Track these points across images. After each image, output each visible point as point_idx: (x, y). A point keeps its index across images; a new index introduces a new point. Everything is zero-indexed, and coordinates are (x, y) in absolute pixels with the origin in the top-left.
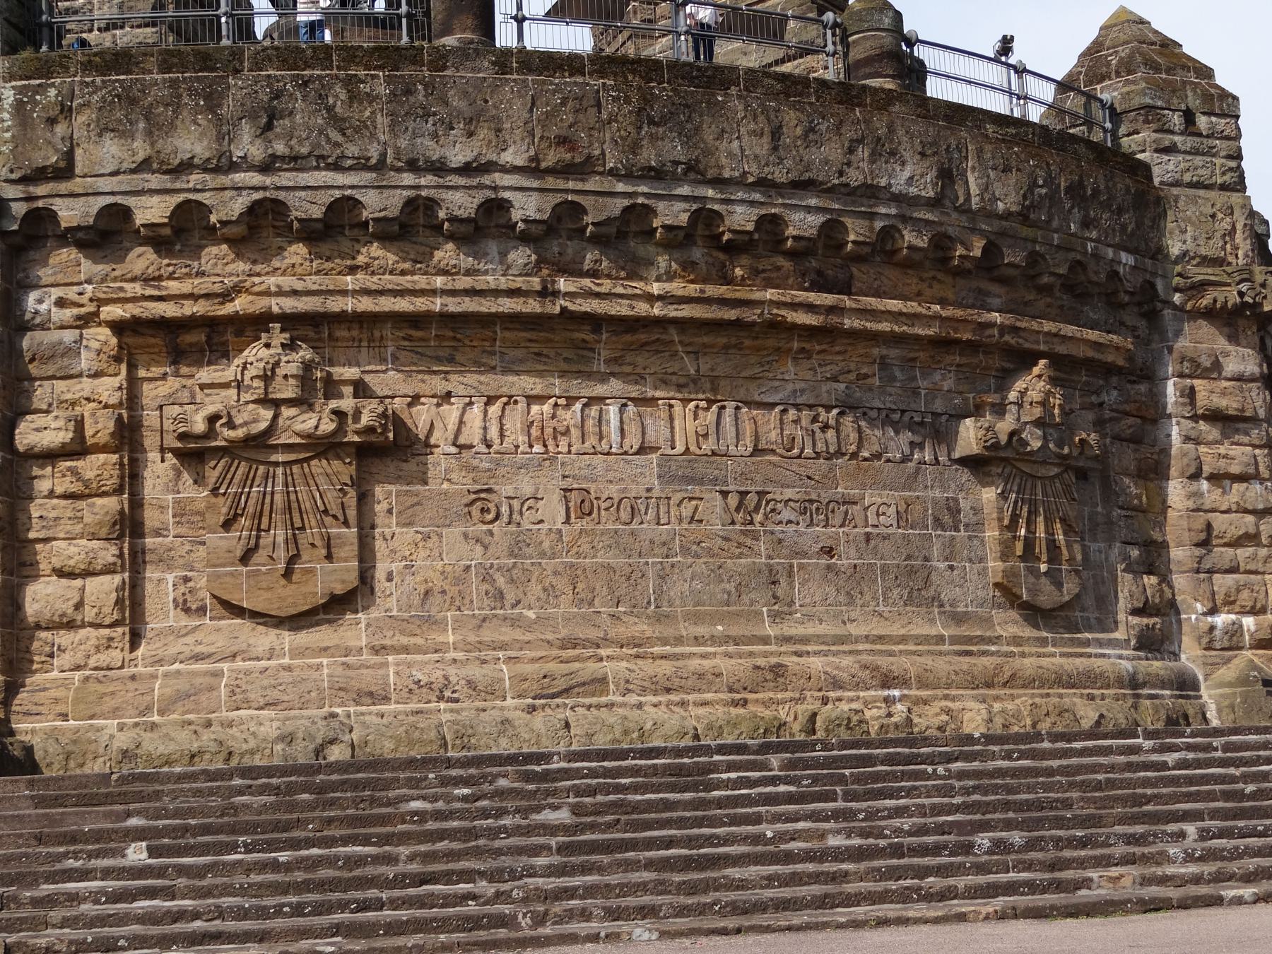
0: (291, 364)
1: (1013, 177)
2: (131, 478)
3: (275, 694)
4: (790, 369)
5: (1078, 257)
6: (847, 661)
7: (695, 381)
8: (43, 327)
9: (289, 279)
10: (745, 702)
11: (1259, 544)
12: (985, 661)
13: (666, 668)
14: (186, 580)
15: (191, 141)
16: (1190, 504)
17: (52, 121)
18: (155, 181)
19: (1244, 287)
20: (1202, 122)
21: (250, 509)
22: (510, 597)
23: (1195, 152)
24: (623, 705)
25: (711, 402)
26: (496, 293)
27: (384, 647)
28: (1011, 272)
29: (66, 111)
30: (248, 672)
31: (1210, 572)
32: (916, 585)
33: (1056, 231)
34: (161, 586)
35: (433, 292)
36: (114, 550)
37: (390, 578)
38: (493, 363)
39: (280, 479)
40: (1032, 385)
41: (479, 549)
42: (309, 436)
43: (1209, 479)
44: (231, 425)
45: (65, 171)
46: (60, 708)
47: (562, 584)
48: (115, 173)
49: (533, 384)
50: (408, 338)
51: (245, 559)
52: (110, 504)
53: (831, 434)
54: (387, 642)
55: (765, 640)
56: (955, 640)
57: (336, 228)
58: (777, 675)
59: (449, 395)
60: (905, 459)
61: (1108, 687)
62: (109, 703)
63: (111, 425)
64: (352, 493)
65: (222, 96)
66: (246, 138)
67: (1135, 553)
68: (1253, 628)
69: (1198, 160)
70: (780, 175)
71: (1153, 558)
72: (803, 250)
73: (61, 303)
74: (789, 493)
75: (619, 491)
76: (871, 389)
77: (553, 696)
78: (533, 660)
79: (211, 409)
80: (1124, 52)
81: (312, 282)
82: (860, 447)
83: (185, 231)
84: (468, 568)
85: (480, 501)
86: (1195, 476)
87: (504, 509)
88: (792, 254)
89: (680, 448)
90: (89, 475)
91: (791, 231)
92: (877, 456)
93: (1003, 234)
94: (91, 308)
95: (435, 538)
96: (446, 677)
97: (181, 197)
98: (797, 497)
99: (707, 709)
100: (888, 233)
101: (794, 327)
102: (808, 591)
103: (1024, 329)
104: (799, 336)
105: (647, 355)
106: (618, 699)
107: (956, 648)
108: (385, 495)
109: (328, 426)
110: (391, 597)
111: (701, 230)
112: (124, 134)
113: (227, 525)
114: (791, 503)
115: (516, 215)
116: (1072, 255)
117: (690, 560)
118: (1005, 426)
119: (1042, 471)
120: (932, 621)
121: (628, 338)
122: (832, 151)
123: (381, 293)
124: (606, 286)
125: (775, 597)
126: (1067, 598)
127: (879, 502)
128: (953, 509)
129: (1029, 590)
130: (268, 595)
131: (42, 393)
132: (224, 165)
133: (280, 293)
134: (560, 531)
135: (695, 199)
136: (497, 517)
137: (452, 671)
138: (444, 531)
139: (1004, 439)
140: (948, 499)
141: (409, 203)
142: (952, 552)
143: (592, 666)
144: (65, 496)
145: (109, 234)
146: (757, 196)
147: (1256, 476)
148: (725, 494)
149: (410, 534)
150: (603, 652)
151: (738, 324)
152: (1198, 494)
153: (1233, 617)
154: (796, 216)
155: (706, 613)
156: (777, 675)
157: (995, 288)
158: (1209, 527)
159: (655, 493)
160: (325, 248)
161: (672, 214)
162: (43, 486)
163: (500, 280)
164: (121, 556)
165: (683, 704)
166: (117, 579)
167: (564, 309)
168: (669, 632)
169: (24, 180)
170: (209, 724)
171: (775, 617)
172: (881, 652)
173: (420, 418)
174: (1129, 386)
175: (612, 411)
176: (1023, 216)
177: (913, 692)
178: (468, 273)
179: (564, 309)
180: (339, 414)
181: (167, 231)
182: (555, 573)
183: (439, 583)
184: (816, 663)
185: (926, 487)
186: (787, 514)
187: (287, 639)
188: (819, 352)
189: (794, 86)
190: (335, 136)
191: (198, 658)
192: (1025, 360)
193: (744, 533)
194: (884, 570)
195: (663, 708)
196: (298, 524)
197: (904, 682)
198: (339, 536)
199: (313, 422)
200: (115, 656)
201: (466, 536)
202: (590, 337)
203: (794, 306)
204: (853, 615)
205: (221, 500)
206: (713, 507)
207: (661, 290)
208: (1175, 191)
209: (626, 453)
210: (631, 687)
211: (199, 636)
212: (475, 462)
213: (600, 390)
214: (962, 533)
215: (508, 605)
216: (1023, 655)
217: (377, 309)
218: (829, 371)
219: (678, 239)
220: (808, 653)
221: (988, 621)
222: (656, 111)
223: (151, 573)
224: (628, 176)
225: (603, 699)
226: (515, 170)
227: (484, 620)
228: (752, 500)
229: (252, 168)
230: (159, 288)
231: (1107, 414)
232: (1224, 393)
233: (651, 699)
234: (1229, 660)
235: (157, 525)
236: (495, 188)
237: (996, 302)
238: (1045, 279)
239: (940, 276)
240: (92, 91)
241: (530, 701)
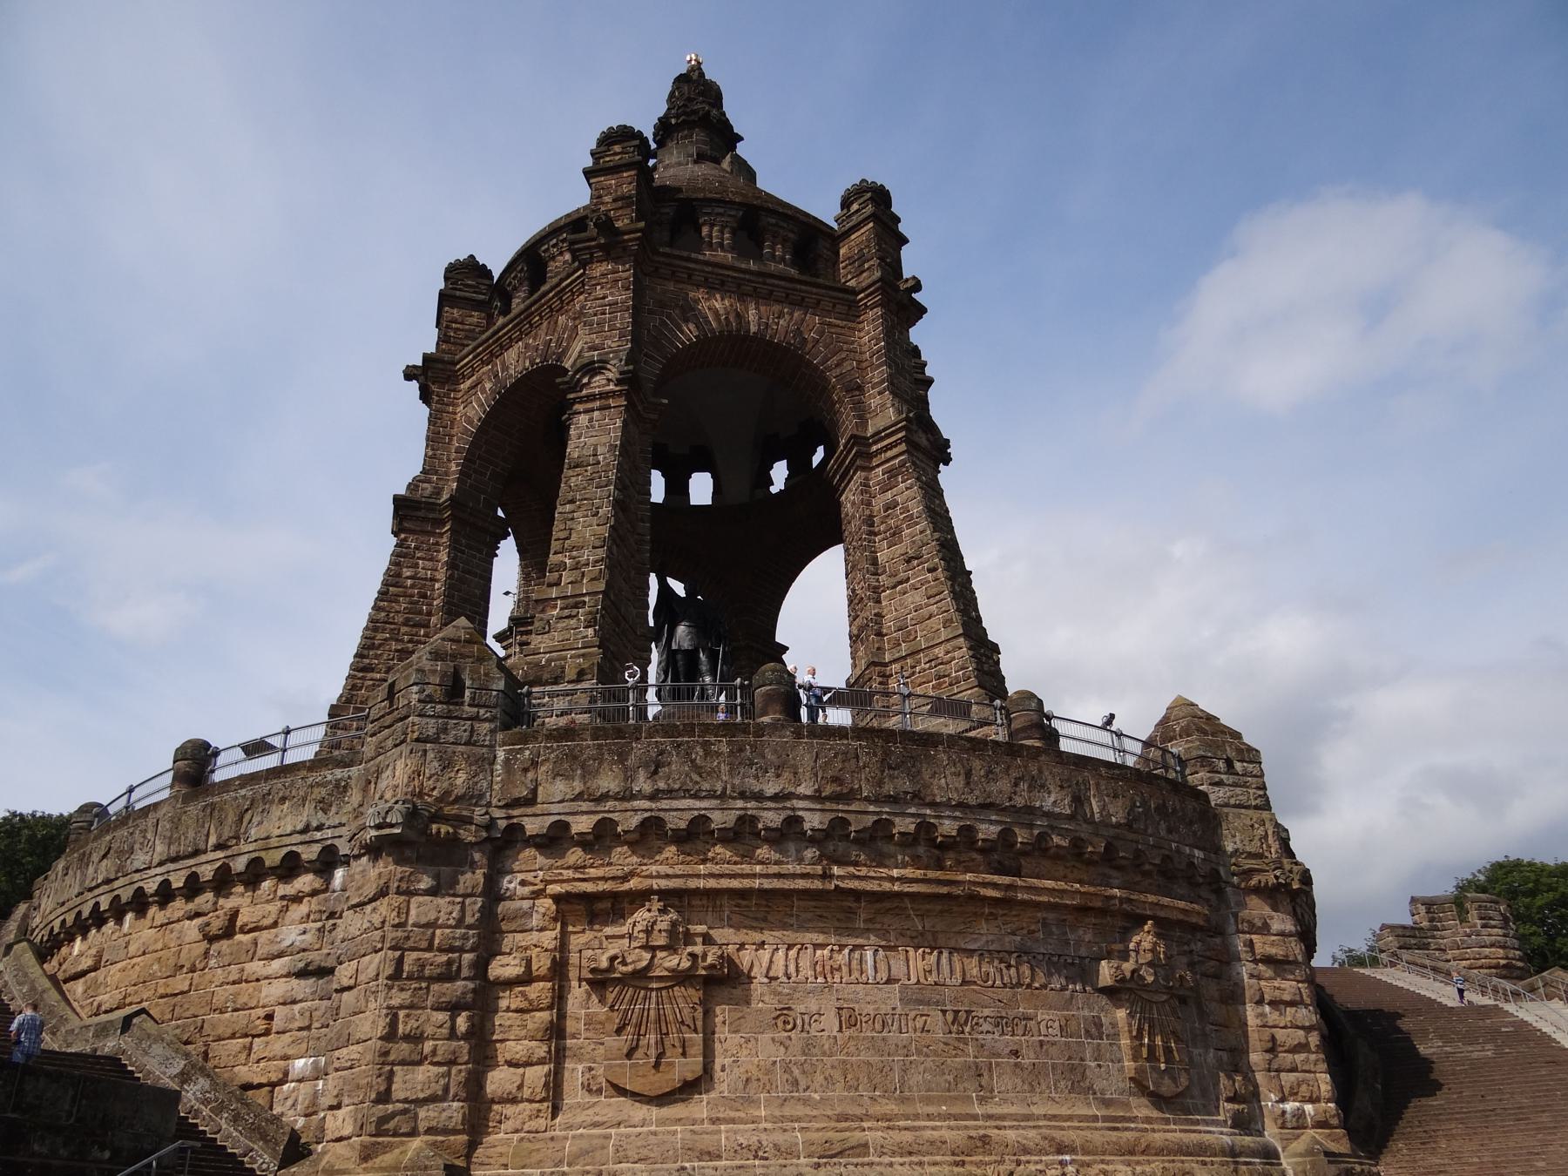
0: (663, 923)
1: (1120, 802)
2: (559, 999)
3: (645, 1152)
4: (984, 927)
6: (1032, 1133)
8: (510, 898)
9: (665, 868)
10: (963, 1163)
11: (1310, 1051)
12: (1128, 1134)
13: (908, 1137)
15: (608, 781)
16: (1258, 1022)
17: (526, 770)
18: (585, 806)
19: (1278, 873)
20: (1238, 766)
22: (802, 1085)
23: (1235, 785)
24: (880, 1164)
25: (933, 949)
26: (794, 876)
28: (1124, 862)
29: (535, 764)
30: (628, 1136)
31: (1278, 1071)
32: (1077, 1080)
34: (575, 1072)
35: (754, 876)
36: (545, 1048)
37: (723, 1070)
39: (654, 1000)
40: (1144, 939)
42: (673, 970)
43: (1271, 1003)
44: (624, 963)
45: (531, 800)
46: (503, 1160)
47: (837, 1075)
48: (562, 801)
49: (820, 938)
50: (738, 906)
51: (629, 1055)
52: (544, 1016)
53: (1013, 970)
54: (721, 1115)
55: (975, 1117)
56: (1106, 1119)
57: (695, 836)
58: (985, 1143)
59: (763, 943)
60: (1063, 989)
62: (536, 1157)
63: (549, 963)
64: (700, 1009)
65: (628, 753)
66: (642, 779)
67: (1225, 1055)
69: (1238, 790)
70: (972, 800)
71: (1236, 1061)
72: (988, 848)
73: (523, 883)
74: (987, 1012)
76: (1037, 940)
78: (818, 1130)
79: (612, 952)
80: (1183, 723)
81: (679, 869)
82: (1033, 980)
83: (602, 838)
85: (783, 1018)
86: (1260, 1002)
87: (799, 1022)
88: (982, 851)
89: (913, 980)
90: (533, 996)
91: (981, 836)
92: (1044, 987)
93: (1117, 837)
94: (541, 886)
97: (600, 816)
100: (1043, 837)
101: (985, 898)
102: (1002, 1082)
108: (722, 1013)
109: (686, 964)
110: (725, 1082)
111: (922, 835)
112: (568, 777)
113: (619, 1031)
115: (807, 826)
118: (1128, 966)
119: (1156, 998)
121: (878, 906)
122: (1004, 785)
123: (721, 876)
124: (864, 871)
127: (1048, 1019)
130: (642, 1080)
131: (508, 942)
132: (627, 796)
133: (659, 876)
135: (919, 815)
137: (763, 1137)
139: (1128, 975)
141: (740, 818)
143: (858, 1134)
144: (516, 1011)
145: (555, 840)
146: (957, 814)
147: (1302, 1002)
148: (944, 1012)
149: (736, 1038)
150: (865, 1125)
151: (949, 896)
152: (1262, 1015)
154: (983, 826)
156: (985, 1143)
157: (1114, 873)
158: (1273, 1038)
159: (898, 1011)
160: (687, 848)
161: (904, 825)
162: (503, 1004)
163: (794, 869)
164: (549, 1052)
165: (921, 1164)
166: (546, 1068)
168: (910, 1110)
169: (507, 806)
171: (982, 1100)
172: (1055, 1127)
173: (745, 958)
175: (869, 954)
176: (1129, 825)
177: (1079, 1157)
178: (777, 863)
180: (693, 956)
183: (755, 1073)
184: (1011, 1135)
186: (986, 1027)
187: (655, 1112)
189: (978, 745)
190: (696, 777)
191: (595, 1125)
192: (1139, 921)
193: (958, 1040)
194: (1054, 1067)
197: (1073, 1151)
200: (541, 1123)
201: (773, 1040)
203: (985, 885)
204: (1035, 1099)
206: (936, 1021)
207: (898, 876)
208: (1226, 810)
211: (597, 1109)
213: (860, 941)
216: (1153, 1130)
218: (1009, 928)
219: (909, 841)
221: (1127, 1105)
222: (893, 760)
223: (569, 1065)
224: (876, 801)
226: (806, 797)
228: (962, 1016)
229: (645, 797)
231: (1196, 958)
232: (1273, 944)
233: (898, 1159)
234: (1298, 1137)
236: (793, 809)
237: (1116, 882)
238: (1147, 867)
240: (551, 752)
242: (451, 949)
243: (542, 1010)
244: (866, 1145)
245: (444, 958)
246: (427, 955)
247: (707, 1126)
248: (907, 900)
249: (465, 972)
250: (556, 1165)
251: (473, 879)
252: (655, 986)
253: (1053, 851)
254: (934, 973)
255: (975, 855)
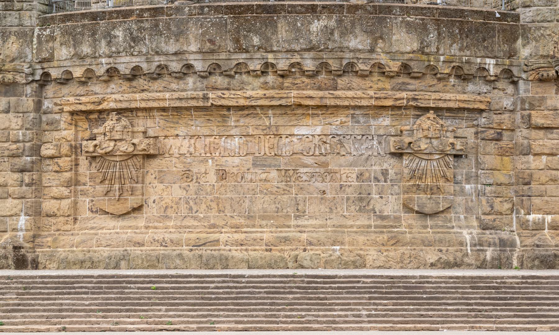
3: (109, 242)
5: (457, 64)
7: (269, 128)
10: (271, 250)
13: (243, 236)
14: (92, 201)
21: (109, 178)
22: (195, 210)
24: (224, 250)
27: (149, 227)
30: (105, 234)
33: (443, 55)
34: (85, 202)
37: (154, 202)
38: (192, 124)
39: (118, 167)
41: (185, 192)
47: (214, 205)
50: (162, 115)
54: (151, 225)
55: (289, 227)
56: (376, 227)
61: (453, 246)
68: (550, 221)
70: (298, 48)
75: (237, 170)
77: (199, 246)
84: (180, 199)
85: (187, 175)
87: (195, 177)
88: (309, 77)
89: (262, 153)
95: (170, 188)
96: (164, 238)
98: (310, 171)
99: (256, 252)
100: (351, 65)
103: (420, 99)
104: (312, 108)
105: (250, 118)
106: (223, 247)
107: (376, 230)
114: (307, 174)
116: (454, 64)
117: (263, 196)
120: (369, 219)
121: (240, 112)
125: (297, 209)
126: (441, 209)
128: (385, 173)
129: (418, 206)
130: (113, 207)
134: (214, 185)
136: (192, 180)
138: (173, 185)
140: (382, 170)
141: (159, 66)
142: (382, 191)
144: (57, 172)
145: (66, 80)
149: (161, 186)
150: (223, 230)
151: (281, 106)
153: (540, 216)
155: (268, 216)
167: (212, 104)
170: (89, 251)
171: (297, 217)
174: (495, 116)
177: (347, 247)
179: (212, 104)
181: (83, 79)
182: (211, 201)
183: (170, 204)
184: (304, 236)
185: (372, 165)
187: (121, 223)
188: (322, 114)
190: (132, 44)
191: (92, 228)
194: (348, 199)
195: (239, 252)
196: (123, 183)
197: (342, 243)
198: (136, 187)
199: (126, 147)
200: (68, 227)
201: (180, 187)
202: (226, 113)
204: (331, 217)
205: (100, 174)
209: (241, 156)
210: (228, 243)
211: (95, 220)
212: (185, 160)
214: (389, 183)
215: (194, 212)
217: (147, 106)
220: (305, 231)
223: (81, 198)
225: (217, 248)
227: (185, 217)
230: (79, 100)
232: (546, 117)
233: (235, 248)
234: (535, 235)
235: (84, 181)
238: (439, 76)
239: (381, 78)
241: (191, 247)
242: (18, 141)
243: (66, 171)
244: (218, 241)
245: (14, 146)
246: (6, 145)
247: (143, 230)
248: (258, 109)
249: (27, 153)
250: (71, 247)
251: (28, 103)
252: (118, 159)
253: (360, 72)
254: (276, 149)
255: (304, 79)
